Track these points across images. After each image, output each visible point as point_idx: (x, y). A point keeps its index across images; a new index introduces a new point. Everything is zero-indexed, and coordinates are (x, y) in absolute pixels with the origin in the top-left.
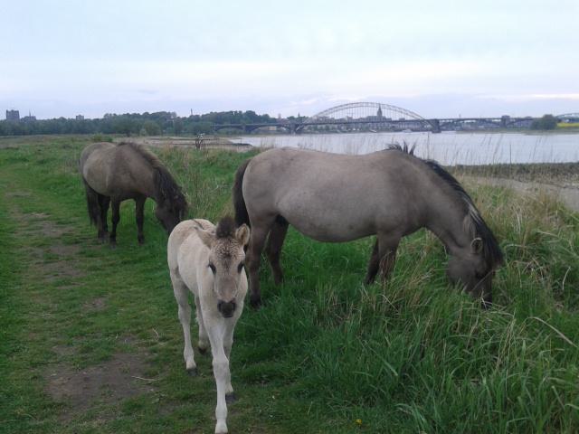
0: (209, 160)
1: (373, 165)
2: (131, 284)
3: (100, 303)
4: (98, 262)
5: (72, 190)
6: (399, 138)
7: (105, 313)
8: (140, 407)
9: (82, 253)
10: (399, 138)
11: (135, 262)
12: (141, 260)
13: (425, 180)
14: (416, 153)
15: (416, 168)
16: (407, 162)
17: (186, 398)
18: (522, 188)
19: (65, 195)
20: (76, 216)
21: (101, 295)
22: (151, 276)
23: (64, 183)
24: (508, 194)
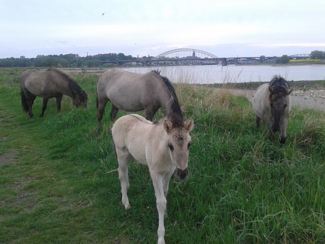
0: (84, 79)
1: (141, 78)
2: (21, 132)
3: (5, 139)
4: (7, 124)
5: (7, 95)
6: (154, 69)
7: (6, 141)
8: (8, 166)
9: (3, 121)
10: (154, 69)
11: (26, 124)
12: (28, 123)
13: (160, 85)
14: (161, 74)
15: (157, 80)
16: (154, 77)
17: (27, 164)
18: (217, 91)
19: (4, 97)
20: (6, 107)
21: (6, 136)
22: (31, 128)
23: (4, 92)
24: (211, 92)
